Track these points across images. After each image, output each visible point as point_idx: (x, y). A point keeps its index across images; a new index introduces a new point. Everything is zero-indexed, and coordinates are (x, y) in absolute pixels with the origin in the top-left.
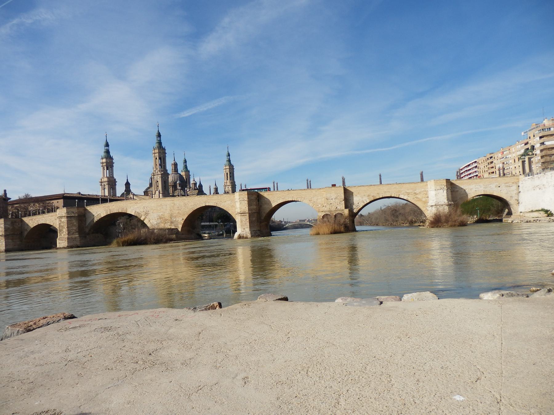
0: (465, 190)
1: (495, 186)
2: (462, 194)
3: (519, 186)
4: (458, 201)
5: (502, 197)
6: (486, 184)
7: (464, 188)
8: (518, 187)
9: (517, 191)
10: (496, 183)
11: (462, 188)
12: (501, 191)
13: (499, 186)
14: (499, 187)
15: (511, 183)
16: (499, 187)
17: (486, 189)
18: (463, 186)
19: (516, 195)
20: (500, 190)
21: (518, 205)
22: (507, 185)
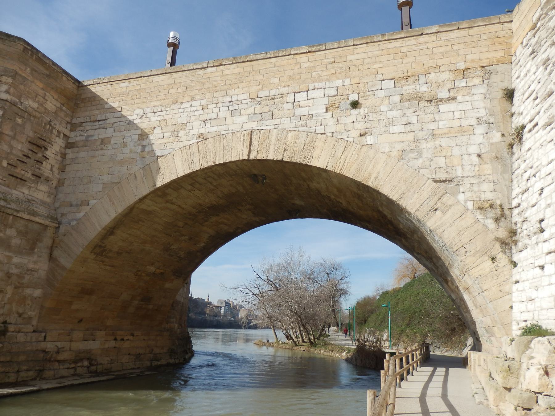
0: (144, 136)
1: (326, 101)
2: (121, 163)
3: (510, 95)
4: (92, 202)
5: (371, 183)
6: (273, 92)
7: (144, 125)
8: (499, 103)
9: (496, 137)
10: (339, 83)
11: (130, 123)
12: (369, 140)
13: (354, 97)
14: (355, 105)
15: (446, 76)
16: (355, 105)
17: (269, 125)
18: (139, 112)
19: (488, 169)
20: (360, 126)
21: (503, 259)
22: (409, 88)
